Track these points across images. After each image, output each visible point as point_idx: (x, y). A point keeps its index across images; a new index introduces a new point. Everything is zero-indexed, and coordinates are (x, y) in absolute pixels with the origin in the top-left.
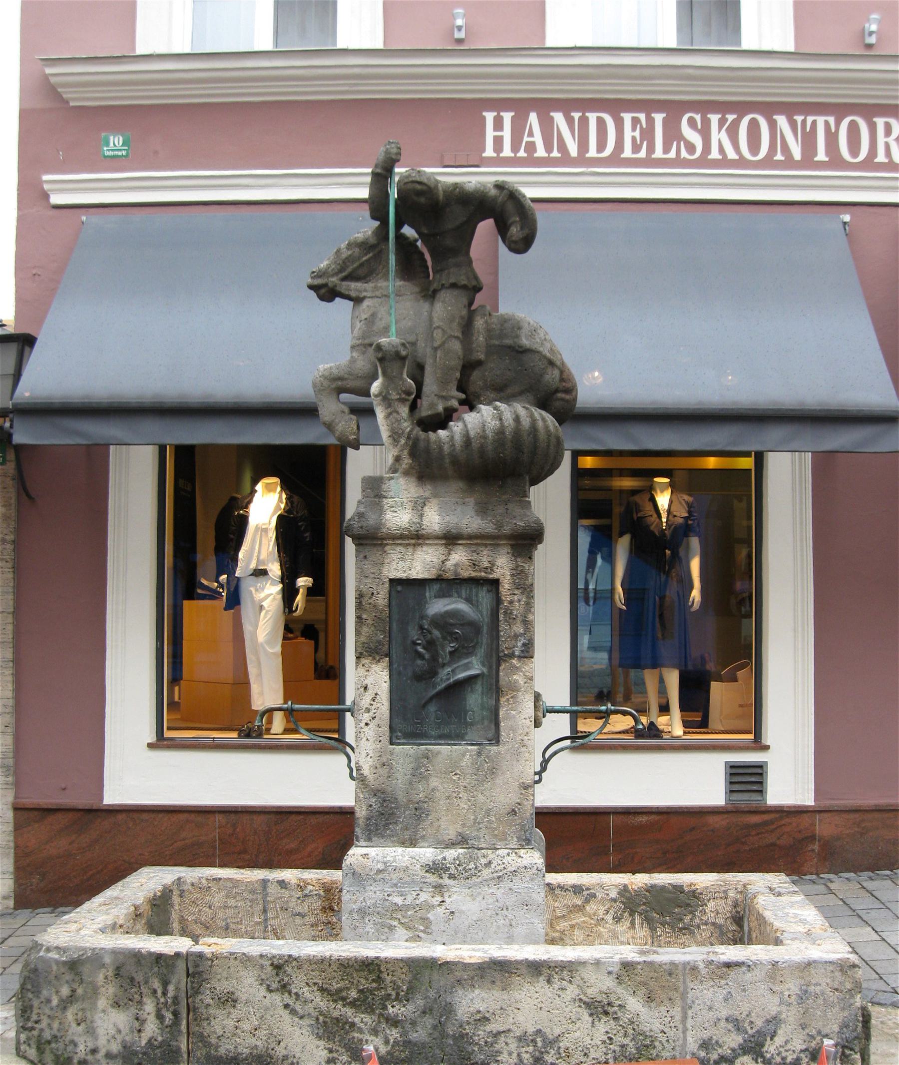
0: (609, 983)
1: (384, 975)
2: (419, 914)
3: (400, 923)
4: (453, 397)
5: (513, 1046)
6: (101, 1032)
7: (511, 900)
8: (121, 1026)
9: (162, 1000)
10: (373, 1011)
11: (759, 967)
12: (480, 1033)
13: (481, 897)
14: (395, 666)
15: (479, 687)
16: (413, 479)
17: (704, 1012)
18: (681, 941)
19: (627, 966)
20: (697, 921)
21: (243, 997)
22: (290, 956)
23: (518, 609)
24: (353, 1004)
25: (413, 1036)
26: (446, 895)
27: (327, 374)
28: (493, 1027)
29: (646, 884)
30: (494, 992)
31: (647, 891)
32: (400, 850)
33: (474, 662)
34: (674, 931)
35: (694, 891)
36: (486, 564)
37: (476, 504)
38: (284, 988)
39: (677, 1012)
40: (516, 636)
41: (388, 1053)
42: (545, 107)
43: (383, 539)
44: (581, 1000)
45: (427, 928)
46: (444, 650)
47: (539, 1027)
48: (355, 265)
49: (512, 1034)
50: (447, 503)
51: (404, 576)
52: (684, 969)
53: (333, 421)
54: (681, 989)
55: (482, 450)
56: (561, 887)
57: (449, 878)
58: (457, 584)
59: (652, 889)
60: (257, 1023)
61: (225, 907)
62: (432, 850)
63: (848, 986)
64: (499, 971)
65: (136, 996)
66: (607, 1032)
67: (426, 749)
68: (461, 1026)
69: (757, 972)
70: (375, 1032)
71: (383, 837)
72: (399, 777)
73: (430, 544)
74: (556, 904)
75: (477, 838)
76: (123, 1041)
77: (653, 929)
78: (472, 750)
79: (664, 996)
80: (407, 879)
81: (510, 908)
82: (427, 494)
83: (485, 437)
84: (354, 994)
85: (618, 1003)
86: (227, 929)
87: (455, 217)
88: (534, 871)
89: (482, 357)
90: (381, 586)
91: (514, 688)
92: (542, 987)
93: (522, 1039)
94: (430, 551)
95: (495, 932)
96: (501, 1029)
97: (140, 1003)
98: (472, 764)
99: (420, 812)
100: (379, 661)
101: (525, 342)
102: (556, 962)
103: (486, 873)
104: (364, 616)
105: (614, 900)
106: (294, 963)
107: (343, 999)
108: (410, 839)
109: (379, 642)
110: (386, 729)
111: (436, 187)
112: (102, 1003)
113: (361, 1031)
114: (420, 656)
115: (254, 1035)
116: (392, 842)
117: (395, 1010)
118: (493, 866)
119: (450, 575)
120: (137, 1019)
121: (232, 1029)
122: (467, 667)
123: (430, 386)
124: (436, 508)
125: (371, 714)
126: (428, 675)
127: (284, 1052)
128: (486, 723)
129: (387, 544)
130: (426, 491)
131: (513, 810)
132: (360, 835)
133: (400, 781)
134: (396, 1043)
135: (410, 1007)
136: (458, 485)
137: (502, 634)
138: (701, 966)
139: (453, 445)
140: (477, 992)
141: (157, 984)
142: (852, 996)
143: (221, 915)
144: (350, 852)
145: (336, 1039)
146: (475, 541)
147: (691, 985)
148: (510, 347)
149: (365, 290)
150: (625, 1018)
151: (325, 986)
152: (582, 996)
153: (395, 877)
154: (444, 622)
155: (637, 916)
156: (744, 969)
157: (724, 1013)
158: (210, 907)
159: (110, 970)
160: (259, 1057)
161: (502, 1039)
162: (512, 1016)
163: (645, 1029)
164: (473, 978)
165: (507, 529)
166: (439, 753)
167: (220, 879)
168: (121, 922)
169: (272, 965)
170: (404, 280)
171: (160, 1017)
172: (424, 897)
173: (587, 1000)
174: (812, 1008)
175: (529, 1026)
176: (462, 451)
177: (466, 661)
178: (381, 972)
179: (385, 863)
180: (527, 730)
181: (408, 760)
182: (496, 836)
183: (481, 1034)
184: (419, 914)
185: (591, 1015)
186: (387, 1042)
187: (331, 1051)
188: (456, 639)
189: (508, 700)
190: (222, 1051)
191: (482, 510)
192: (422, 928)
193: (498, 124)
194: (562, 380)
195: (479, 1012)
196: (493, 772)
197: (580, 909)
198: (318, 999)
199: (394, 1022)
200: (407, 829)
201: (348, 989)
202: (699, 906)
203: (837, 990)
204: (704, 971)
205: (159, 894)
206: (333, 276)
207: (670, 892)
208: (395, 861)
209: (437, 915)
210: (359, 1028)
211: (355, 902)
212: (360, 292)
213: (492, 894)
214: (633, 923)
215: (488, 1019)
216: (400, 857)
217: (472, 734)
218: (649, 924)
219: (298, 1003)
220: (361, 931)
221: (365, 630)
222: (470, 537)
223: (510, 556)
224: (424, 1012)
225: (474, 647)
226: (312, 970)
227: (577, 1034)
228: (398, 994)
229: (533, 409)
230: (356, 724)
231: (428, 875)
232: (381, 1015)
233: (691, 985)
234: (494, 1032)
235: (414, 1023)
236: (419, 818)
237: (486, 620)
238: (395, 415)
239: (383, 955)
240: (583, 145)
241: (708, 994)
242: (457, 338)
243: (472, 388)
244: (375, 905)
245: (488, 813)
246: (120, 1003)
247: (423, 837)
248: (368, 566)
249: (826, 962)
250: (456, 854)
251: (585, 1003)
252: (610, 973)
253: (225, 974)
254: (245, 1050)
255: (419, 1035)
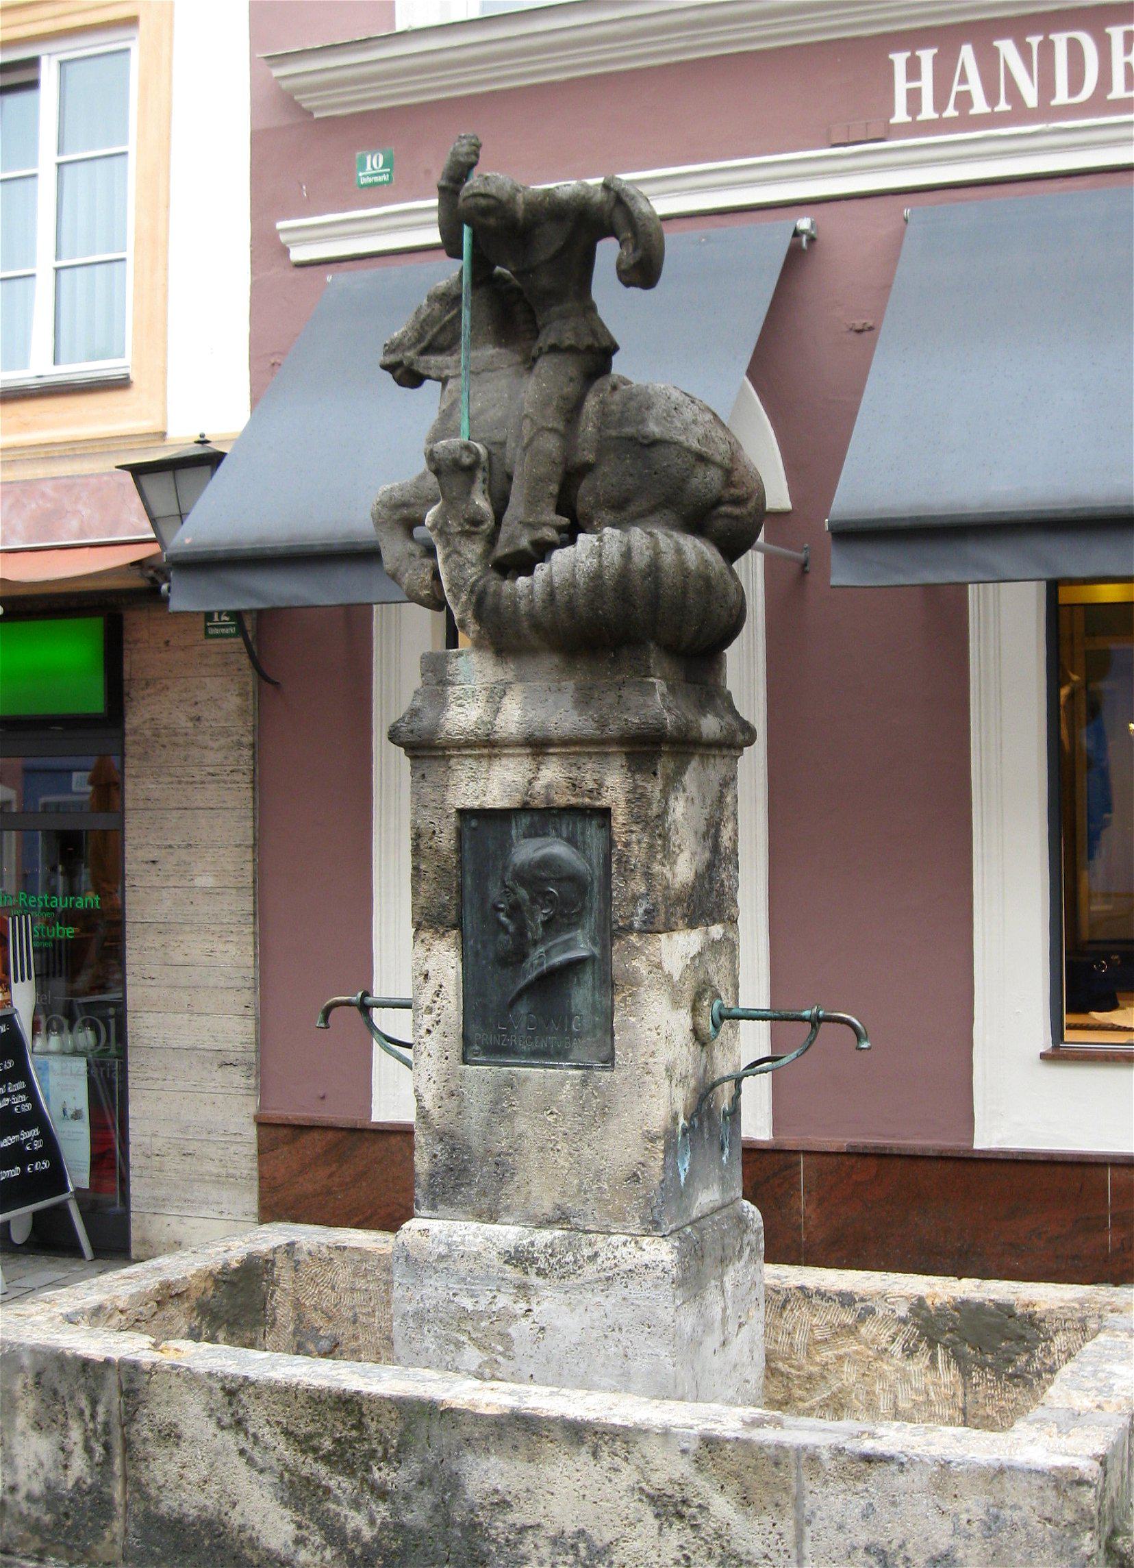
0: (682, 1468)
1: (367, 1420)
2: (498, 1326)
3: (471, 1339)
4: (545, 524)
5: (545, 1551)
6: (20, 1462)
7: (625, 1317)
8: (44, 1457)
9: (91, 1426)
10: (352, 1474)
11: (920, 1466)
12: (498, 1524)
13: (582, 1308)
14: (471, 943)
15: (588, 977)
16: (489, 655)
17: (831, 1532)
18: (1011, 1396)
19: (710, 1443)
20: (1036, 1365)
21: (188, 1433)
22: (246, 1378)
23: (637, 854)
24: (326, 1459)
25: (407, 1518)
26: (534, 1300)
27: (385, 499)
28: (517, 1517)
29: (954, 1299)
30: (518, 1463)
31: (956, 1309)
32: (474, 1225)
33: (580, 938)
34: (999, 1378)
35: (1030, 1316)
36: (591, 785)
37: (577, 689)
38: (239, 1424)
39: (787, 1527)
40: (635, 899)
41: (375, 1539)
42: (983, 33)
43: (445, 748)
44: (641, 1489)
45: (507, 1349)
46: (534, 920)
47: (581, 1526)
48: (435, 330)
49: (543, 1533)
50: (535, 690)
51: (476, 804)
52: (798, 1458)
53: (397, 570)
54: (794, 1490)
55: (570, 607)
56: (822, 1294)
57: (538, 1274)
58: (554, 815)
59: (963, 1306)
60: (206, 1473)
61: (353, 1290)
62: (518, 1229)
63: (1069, 1515)
64: (522, 1431)
65: (60, 1416)
66: (681, 1546)
67: (510, 1072)
68: (472, 1511)
69: (914, 1474)
70: (356, 1505)
71: (452, 1204)
72: (474, 1115)
73: (512, 755)
74: (815, 1321)
75: (582, 1215)
76: (46, 1480)
77: (965, 1374)
78: (574, 1077)
79: (767, 1499)
80: (478, 1272)
81: (624, 1330)
82: (509, 676)
83: (574, 585)
84: (327, 1444)
85: (697, 1501)
86: (354, 1322)
87: (550, 241)
88: (659, 1273)
89: (590, 457)
90: (444, 821)
91: (633, 980)
92: (585, 1464)
93: (556, 1541)
94: (511, 766)
95: (603, 1365)
96: (529, 1522)
97: (65, 1426)
98: (574, 1098)
99: (502, 1170)
100: (443, 935)
101: (654, 428)
102: (605, 1425)
103: (589, 1270)
104: (423, 867)
105: (904, 1321)
106: (251, 1390)
107: (315, 1450)
108: (489, 1209)
109: (444, 906)
110: (455, 1041)
111: (512, 199)
112: (21, 1422)
113: (339, 1503)
114: (504, 928)
115: (203, 1490)
116: (465, 1212)
117: (382, 1474)
118: (599, 1260)
119: (539, 803)
120: (63, 1449)
121: (175, 1477)
122: (568, 946)
123: (516, 509)
124: (519, 699)
125: (434, 1016)
126: (516, 957)
127: (240, 1521)
128: (599, 1034)
129: (451, 756)
130: (506, 672)
131: (635, 1174)
132: (421, 1200)
133: (475, 1119)
134: (384, 1525)
135: (403, 1473)
136: (550, 661)
137: (614, 894)
138: (825, 1455)
139: (532, 601)
140: (493, 1459)
141: (84, 1403)
142: (1076, 1534)
143: (347, 1301)
144: (406, 1225)
145: (307, 1510)
146: (573, 749)
147: (809, 1485)
148: (631, 439)
149: (448, 367)
150: (709, 1528)
151: (291, 1428)
152: (643, 1485)
153: (462, 1267)
154: (538, 877)
155: (940, 1350)
156: (894, 1467)
157: (863, 1538)
158: (333, 1288)
159: (30, 1376)
160: (209, 1523)
161: (529, 1538)
162: (543, 1503)
163: (739, 1549)
164: (487, 1438)
165: (613, 730)
166: (527, 1079)
167: (345, 1248)
168: (121, 1305)
169: (223, 1388)
170: (500, 345)
171: (88, 1450)
172: (503, 1300)
173: (652, 1492)
174: (1006, 1546)
175: (568, 1523)
176: (545, 608)
177: (566, 937)
178: (363, 1415)
179: (449, 1245)
180: (652, 1048)
181: (484, 1088)
182: (608, 1213)
183: (500, 1526)
184: (498, 1326)
185: (657, 1516)
186: (372, 1522)
187: (300, 1527)
188: (551, 901)
189: (624, 999)
190: (163, 1509)
191: (584, 700)
192: (500, 1348)
193: (913, 71)
194: (729, 482)
195: (496, 1491)
196: (604, 1112)
197: (852, 1331)
198: (282, 1447)
199: (382, 1494)
200: (485, 1194)
201: (321, 1435)
202: (1039, 1340)
203: (1049, 1520)
204: (830, 1465)
205: (235, 1265)
206: (409, 348)
207: (992, 1314)
208: (462, 1243)
209: (521, 1329)
210: (336, 1496)
211: (410, 1301)
212: (441, 369)
213: (598, 1304)
214: (933, 1359)
215: (509, 1505)
216: (471, 1238)
217: (579, 1052)
218: (958, 1363)
219: (257, 1449)
220: (418, 1345)
221: (424, 886)
222: (565, 743)
223: (624, 770)
224: (421, 1483)
225: (579, 914)
226: (274, 1402)
227: (638, 1544)
228: (386, 1451)
229: (675, 534)
230: (414, 1030)
231: (507, 1267)
232: (364, 1480)
233: (809, 1485)
234: (518, 1526)
235: (407, 1498)
236: (501, 1180)
237: (597, 873)
238: (455, 557)
239: (366, 1389)
240: (1046, 87)
241: (837, 1503)
242: (553, 430)
243: (581, 508)
244: (436, 1307)
245: (598, 1176)
246: (42, 1424)
247: (507, 1208)
248: (427, 789)
249: (1030, 1471)
250: (550, 1237)
251: (648, 1496)
252: (684, 1452)
253: (165, 1397)
254: (192, 1511)
255: (416, 1516)
